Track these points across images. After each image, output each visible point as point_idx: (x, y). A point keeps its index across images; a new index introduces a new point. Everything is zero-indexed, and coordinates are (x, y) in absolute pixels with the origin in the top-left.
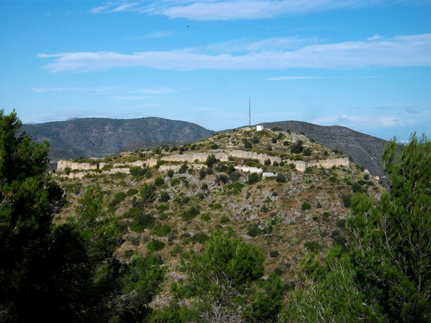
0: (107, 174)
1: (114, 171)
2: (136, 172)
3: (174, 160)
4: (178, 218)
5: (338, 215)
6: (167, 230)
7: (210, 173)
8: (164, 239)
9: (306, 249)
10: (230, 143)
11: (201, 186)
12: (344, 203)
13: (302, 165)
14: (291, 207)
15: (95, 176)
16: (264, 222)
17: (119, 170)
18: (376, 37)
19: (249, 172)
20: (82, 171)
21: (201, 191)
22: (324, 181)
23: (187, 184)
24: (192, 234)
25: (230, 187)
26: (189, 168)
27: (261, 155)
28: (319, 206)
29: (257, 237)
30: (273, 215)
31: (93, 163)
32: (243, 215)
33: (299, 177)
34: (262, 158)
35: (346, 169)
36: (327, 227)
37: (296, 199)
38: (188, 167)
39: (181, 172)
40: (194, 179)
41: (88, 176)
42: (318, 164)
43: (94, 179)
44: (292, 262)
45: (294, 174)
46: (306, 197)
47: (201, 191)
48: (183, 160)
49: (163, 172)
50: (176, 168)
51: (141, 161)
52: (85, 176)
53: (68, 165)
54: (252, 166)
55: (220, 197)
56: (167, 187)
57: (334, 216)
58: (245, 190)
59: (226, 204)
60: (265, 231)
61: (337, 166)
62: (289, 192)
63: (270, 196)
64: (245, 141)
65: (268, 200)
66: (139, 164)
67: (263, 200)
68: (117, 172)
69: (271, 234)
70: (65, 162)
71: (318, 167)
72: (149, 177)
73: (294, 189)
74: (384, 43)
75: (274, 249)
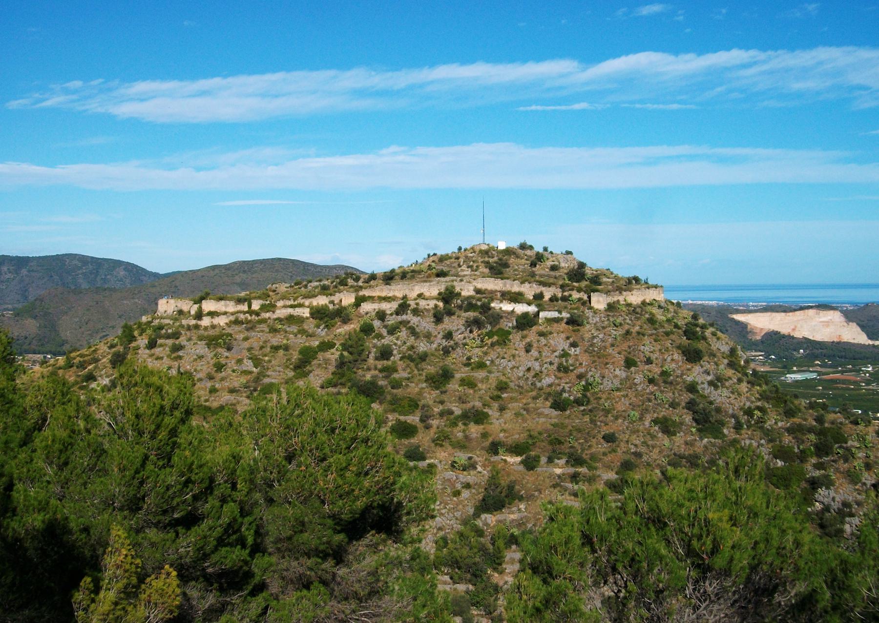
0: (269, 318)
1: (281, 313)
2: (319, 314)
3: (383, 294)
4: (420, 386)
5: (682, 374)
6: (414, 405)
7: (450, 313)
8: (413, 419)
9: (657, 428)
10: (464, 267)
11: (442, 333)
12: (685, 355)
13: (601, 299)
14: (607, 364)
15: (248, 322)
16: (570, 388)
17: (290, 311)
18: (394, 148)
19: (513, 311)
20: (225, 313)
21: (445, 343)
22: (639, 323)
23: (413, 332)
24: (458, 412)
25: (490, 335)
26: (412, 307)
27: (527, 285)
28: (649, 361)
29: (568, 412)
30: (580, 377)
31: (240, 301)
32: (528, 378)
33: (600, 318)
34: (529, 290)
35: (662, 304)
36: (674, 393)
37: (610, 350)
38: (409, 305)
39: (397, 313)
40: (425, 324)
41: (237, 322)
42: (621, 298)
43: (249, 326)
44: (643, 449)
45: (591, 314)
46: (624, 346)
47: (445, 343)
48: (400, 295)
49: (367, 313)
50: (389, 307)
51: (325, 297)
52: (230, 322)
53: (179, 305)
54: (519, 303)
55: (477, 351)
56: (380, 336)
57: (677, 377)
58: (516, 338)
59: (492, 361)
60: (578, 402)
61: (648, 301)
62: (595, 341)
63: (566, 348)
64: (487, 264)
65: (565, 354)
66: (321, 301)
67: (556, 354)
68: (286, 314)
69: (590, 407)
70: (172, 301)
71: (622, 302)
72: (346, 320)
73: (601, 336)
74: (401, 158)
75: (605, 430)
